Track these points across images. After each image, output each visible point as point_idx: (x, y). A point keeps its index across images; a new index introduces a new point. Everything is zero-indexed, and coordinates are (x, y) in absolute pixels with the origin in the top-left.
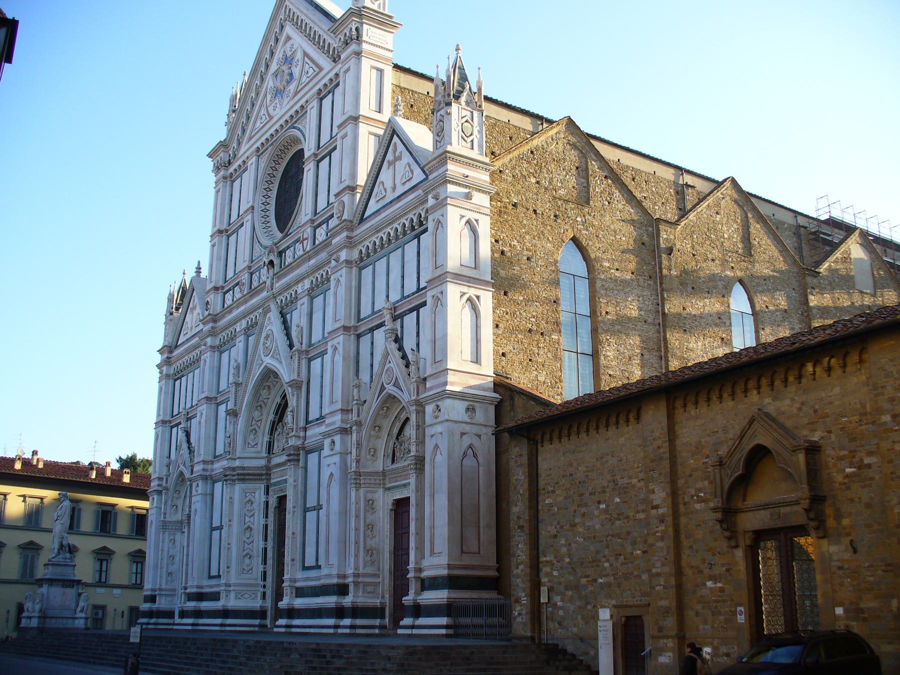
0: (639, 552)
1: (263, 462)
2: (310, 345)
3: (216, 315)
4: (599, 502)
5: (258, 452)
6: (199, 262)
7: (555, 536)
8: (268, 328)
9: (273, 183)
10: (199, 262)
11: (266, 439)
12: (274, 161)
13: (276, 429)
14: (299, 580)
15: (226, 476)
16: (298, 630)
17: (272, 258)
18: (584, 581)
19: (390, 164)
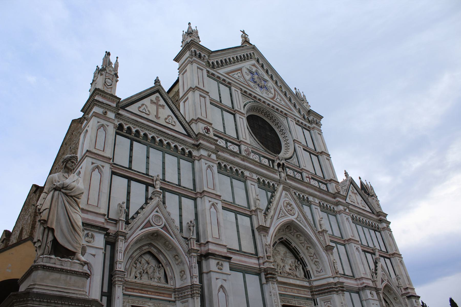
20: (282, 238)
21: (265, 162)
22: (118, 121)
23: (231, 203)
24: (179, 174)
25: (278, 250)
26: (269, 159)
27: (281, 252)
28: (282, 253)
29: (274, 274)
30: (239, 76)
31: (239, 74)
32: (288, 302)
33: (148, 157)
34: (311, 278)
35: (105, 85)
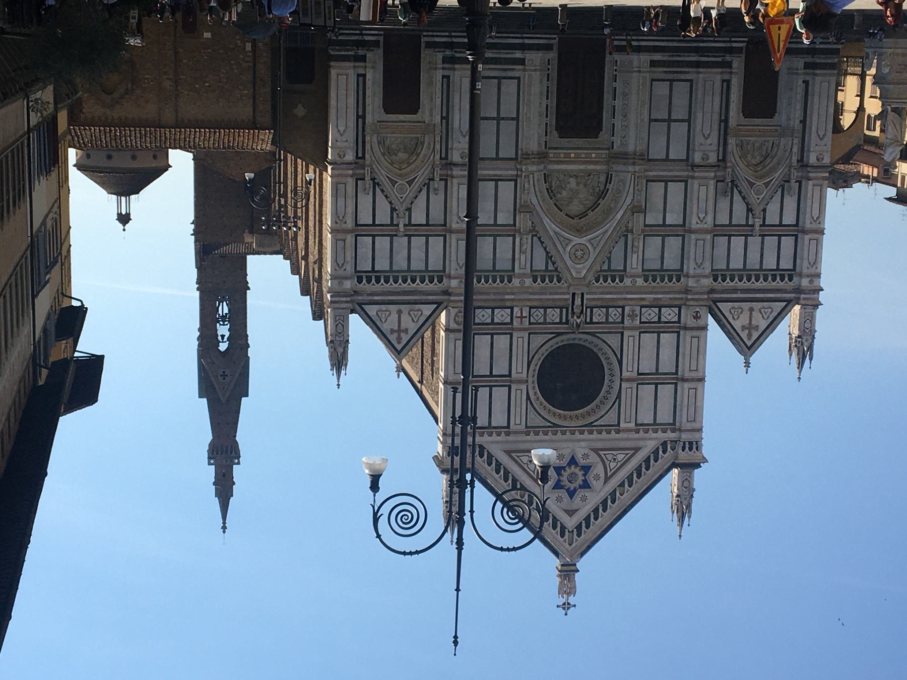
0: (184, 61)
1: (615, 167)
2: (514, 236)
3: (685, 305)
4: (210, 87)
5: (616, 176)
6: (747, 373)
7: (240, 74)
8: (581, 266)
9: (604, 397)
10: (747, 373)
11: (609, 186)
12: (595, 412)
13: (602, 193)
14: (519, 70)
15: (642, 159)
16: (443, 34)
17: (572, 320)
18: (221, 51)
19: (406, 331)
20: (580, 219)
21: (599, 315)
22: (794, 283)
23: (669, 236)
24: (729, 250)
25: (581, 206)
26: (591, 322)
27: (577, 204)
28: (576, 202)
29: (639, 159)
30: (615, 459)
31: (613, 465)
32: (588, 141)
33: (762, 255)
34: (545, 174)
35: (811, 318)
